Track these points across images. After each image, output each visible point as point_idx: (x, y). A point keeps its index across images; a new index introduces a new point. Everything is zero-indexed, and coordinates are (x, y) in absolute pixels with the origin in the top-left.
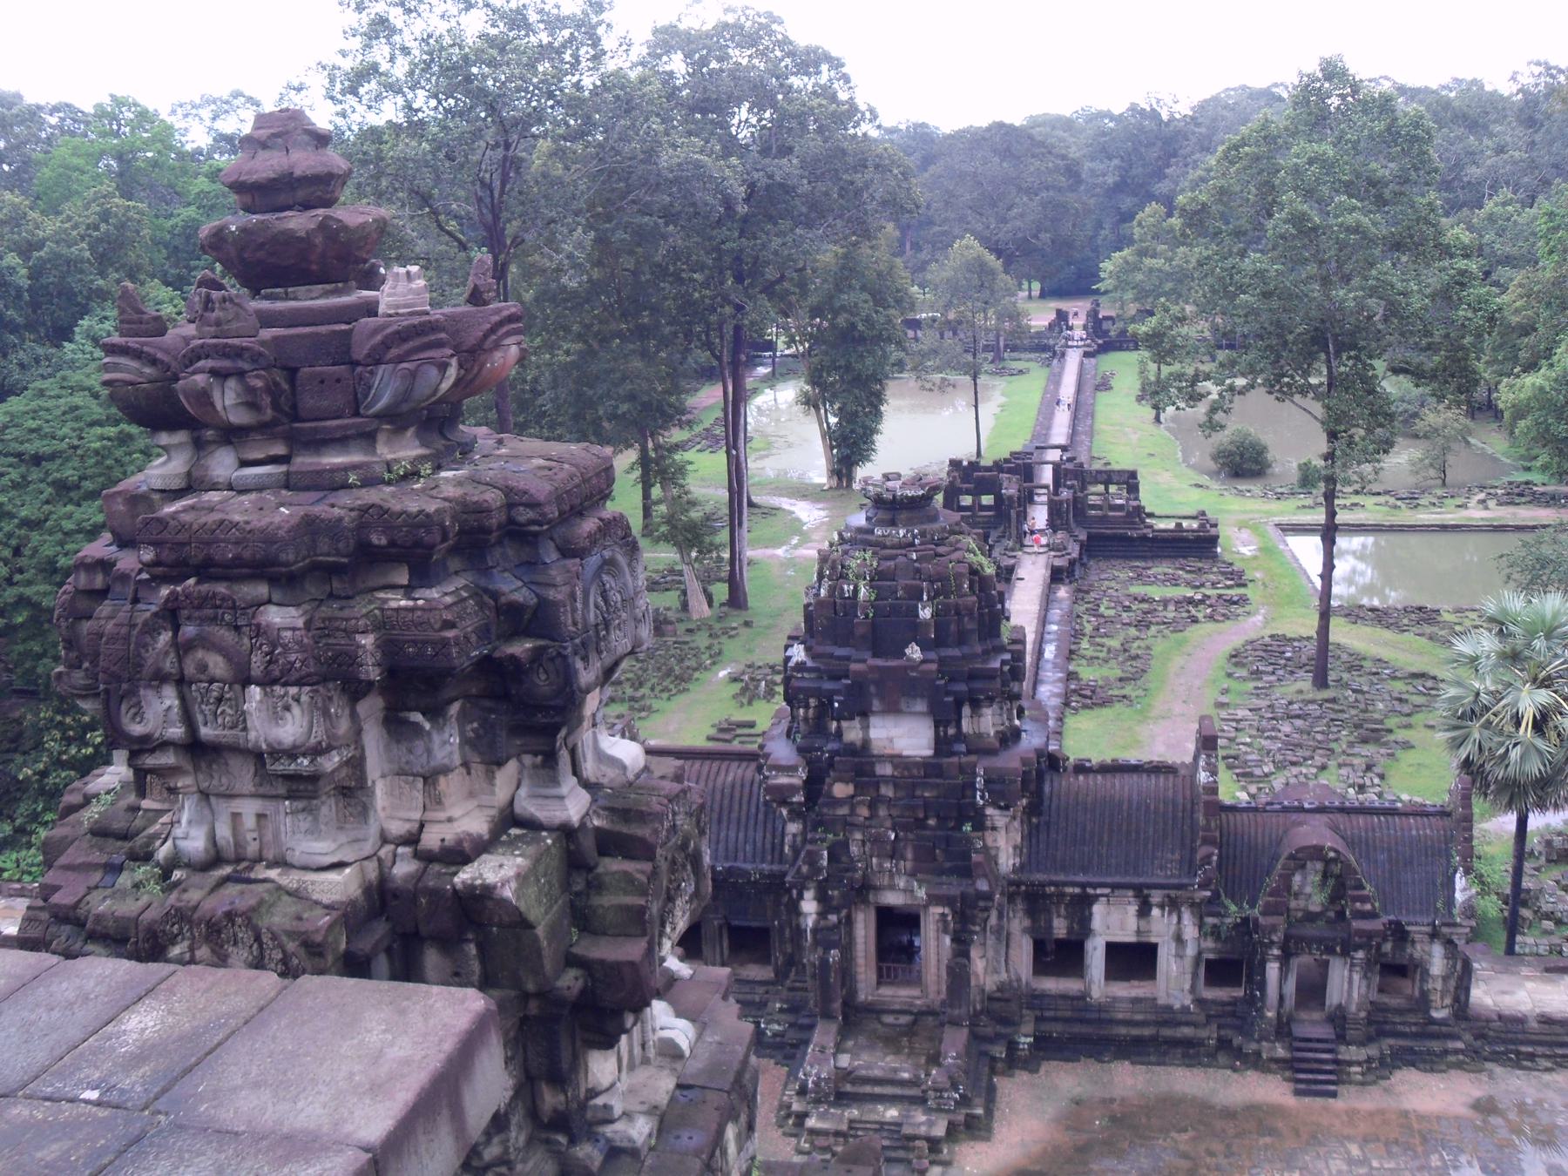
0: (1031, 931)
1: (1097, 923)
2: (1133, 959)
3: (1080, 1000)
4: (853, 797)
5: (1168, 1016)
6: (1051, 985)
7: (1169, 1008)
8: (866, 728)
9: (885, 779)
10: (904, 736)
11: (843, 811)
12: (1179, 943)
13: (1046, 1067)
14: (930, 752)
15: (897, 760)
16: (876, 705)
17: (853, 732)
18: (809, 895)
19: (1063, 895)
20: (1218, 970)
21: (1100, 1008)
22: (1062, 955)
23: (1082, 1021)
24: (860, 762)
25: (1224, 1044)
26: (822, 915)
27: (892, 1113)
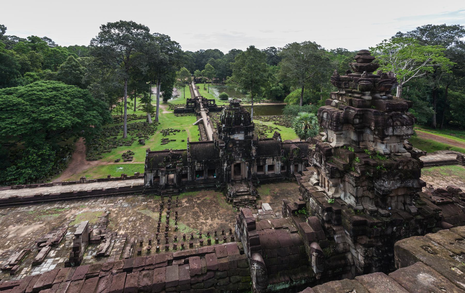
0: (257, 165)
1: (267, 162)
2: (271, 167)
3: (264, 175)
5: (277, 176)
6: (260, 173)
7: (277, 174)
9: (238, 144)
10: (239, 137)
12: (278, 166)
13: (262, 186)
15: (239, 140)
17: (232, 137)
18: (226, 163)
20: (282, 168)
21: (268, 175)
22: (260, 168)
23: (265, 178)
24: (233, 141)
25: (286, 179)
26: (227, 166)
27: (246, 197)
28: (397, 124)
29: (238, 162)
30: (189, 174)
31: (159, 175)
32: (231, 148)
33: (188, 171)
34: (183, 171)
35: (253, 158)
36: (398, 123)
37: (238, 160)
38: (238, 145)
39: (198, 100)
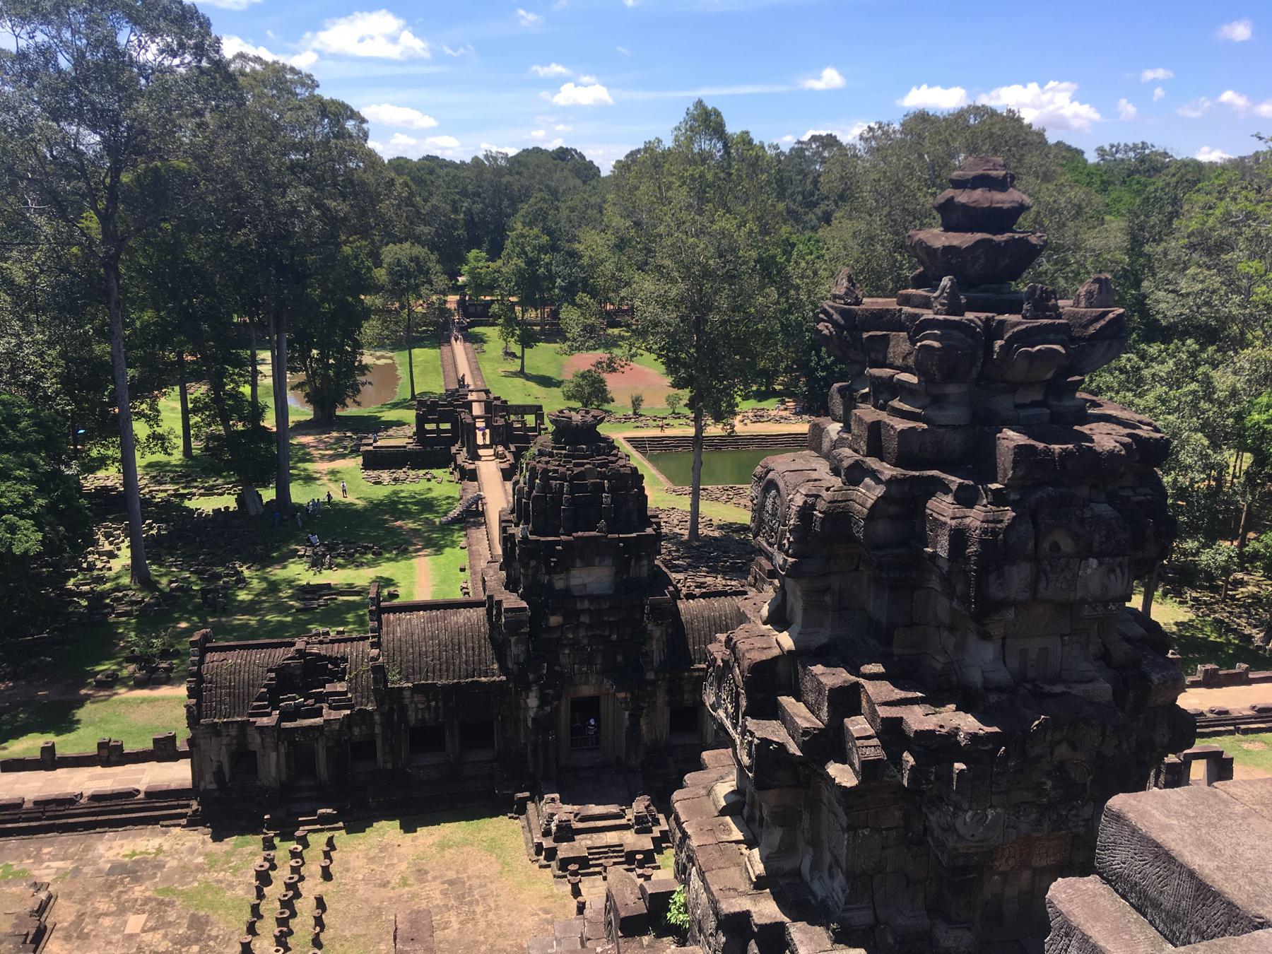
4: (563, 625)
8: (567, 579)
11: (557, 635)
14: (611, 592)
15: (592, 598)
16: (578, 563)
19: (691, 677)
26: (540, 707)
28: (1056, 547)
29: (586, 691)
30: (379, 741)
31: (252, 748)
32: (556, 628)
33: (378, 730)
34: (356, 731)
35: (651, 676)
36: (1067, 545)
37: (587, 683)
38: (585, 619)
39: (468, 405)
